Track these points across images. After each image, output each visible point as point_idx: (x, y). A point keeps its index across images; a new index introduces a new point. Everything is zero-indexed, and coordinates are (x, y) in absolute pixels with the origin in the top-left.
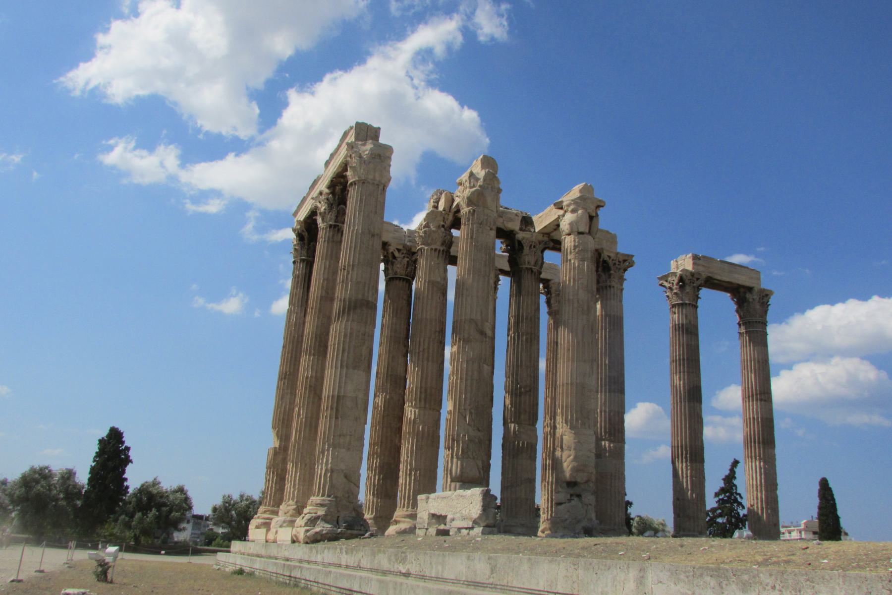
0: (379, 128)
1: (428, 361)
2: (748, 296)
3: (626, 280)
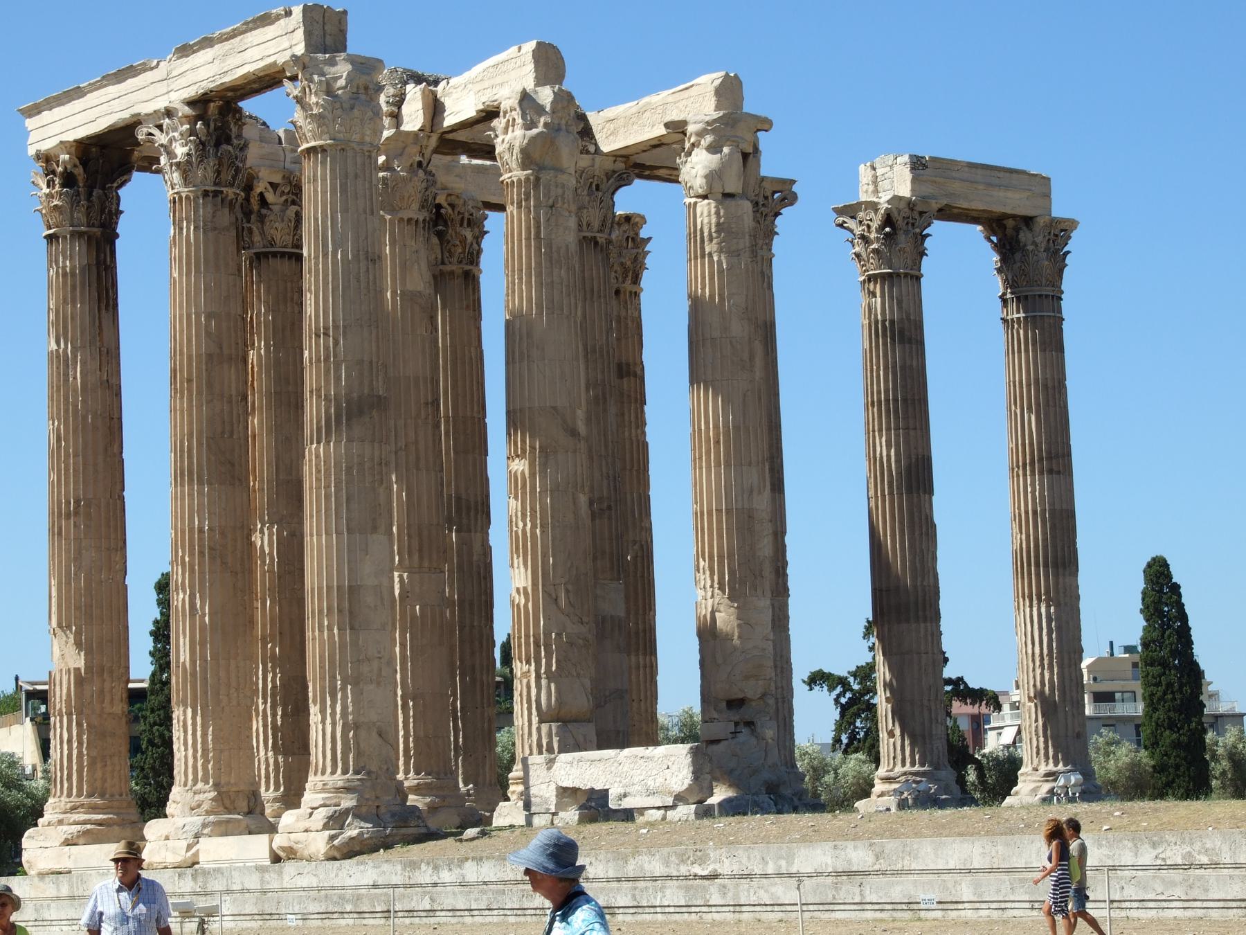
0: (345, 12)
1: (418, 469)
2: (1024, 236)
3: (777, 234)
